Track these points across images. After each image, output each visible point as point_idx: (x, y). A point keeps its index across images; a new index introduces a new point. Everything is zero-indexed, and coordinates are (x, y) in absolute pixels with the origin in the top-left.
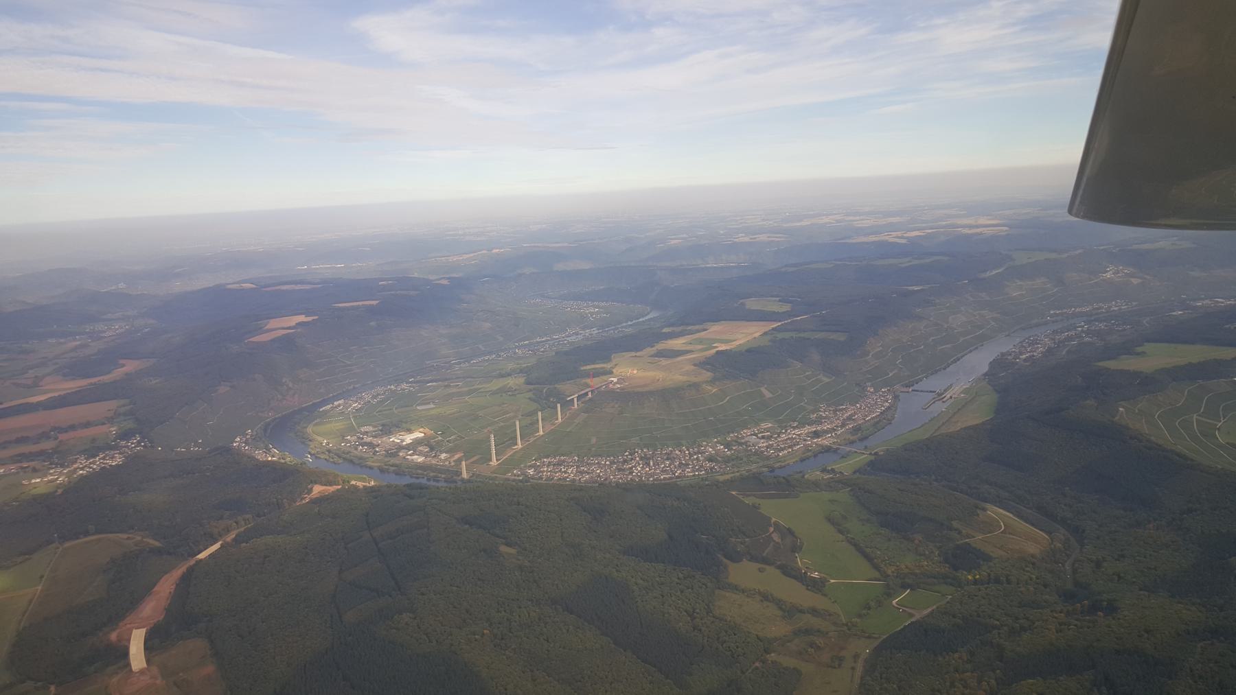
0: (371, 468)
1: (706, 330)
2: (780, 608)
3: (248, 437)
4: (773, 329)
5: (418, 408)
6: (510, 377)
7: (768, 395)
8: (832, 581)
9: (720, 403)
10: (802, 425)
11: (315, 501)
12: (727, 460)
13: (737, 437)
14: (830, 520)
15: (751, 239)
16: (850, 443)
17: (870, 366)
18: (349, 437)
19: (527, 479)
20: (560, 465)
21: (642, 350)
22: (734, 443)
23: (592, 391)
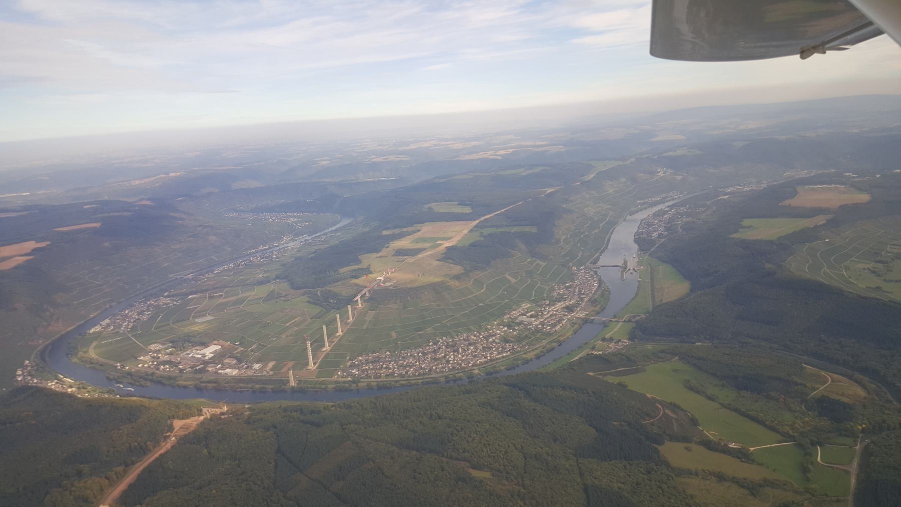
0: (185, 387)
1: (419, 231)
2: (743, 487)
3: (29, 368)
4: (475, 227)
5: (197, 320)
6: (269, 283)
7: (513, 280)
8: (752, 449)
9: (483, 291)
10: (553, 302)
11: (183, 441)
12: (519, 339)
13: (510, 318)
14: (691, 388)
15: (384, 159)
16: (598, 314)
17: (565, 251)
18: (142, 358)
20: (379, 362)
21: (380, 251)
22: (513, 324)
23: (369, 291)
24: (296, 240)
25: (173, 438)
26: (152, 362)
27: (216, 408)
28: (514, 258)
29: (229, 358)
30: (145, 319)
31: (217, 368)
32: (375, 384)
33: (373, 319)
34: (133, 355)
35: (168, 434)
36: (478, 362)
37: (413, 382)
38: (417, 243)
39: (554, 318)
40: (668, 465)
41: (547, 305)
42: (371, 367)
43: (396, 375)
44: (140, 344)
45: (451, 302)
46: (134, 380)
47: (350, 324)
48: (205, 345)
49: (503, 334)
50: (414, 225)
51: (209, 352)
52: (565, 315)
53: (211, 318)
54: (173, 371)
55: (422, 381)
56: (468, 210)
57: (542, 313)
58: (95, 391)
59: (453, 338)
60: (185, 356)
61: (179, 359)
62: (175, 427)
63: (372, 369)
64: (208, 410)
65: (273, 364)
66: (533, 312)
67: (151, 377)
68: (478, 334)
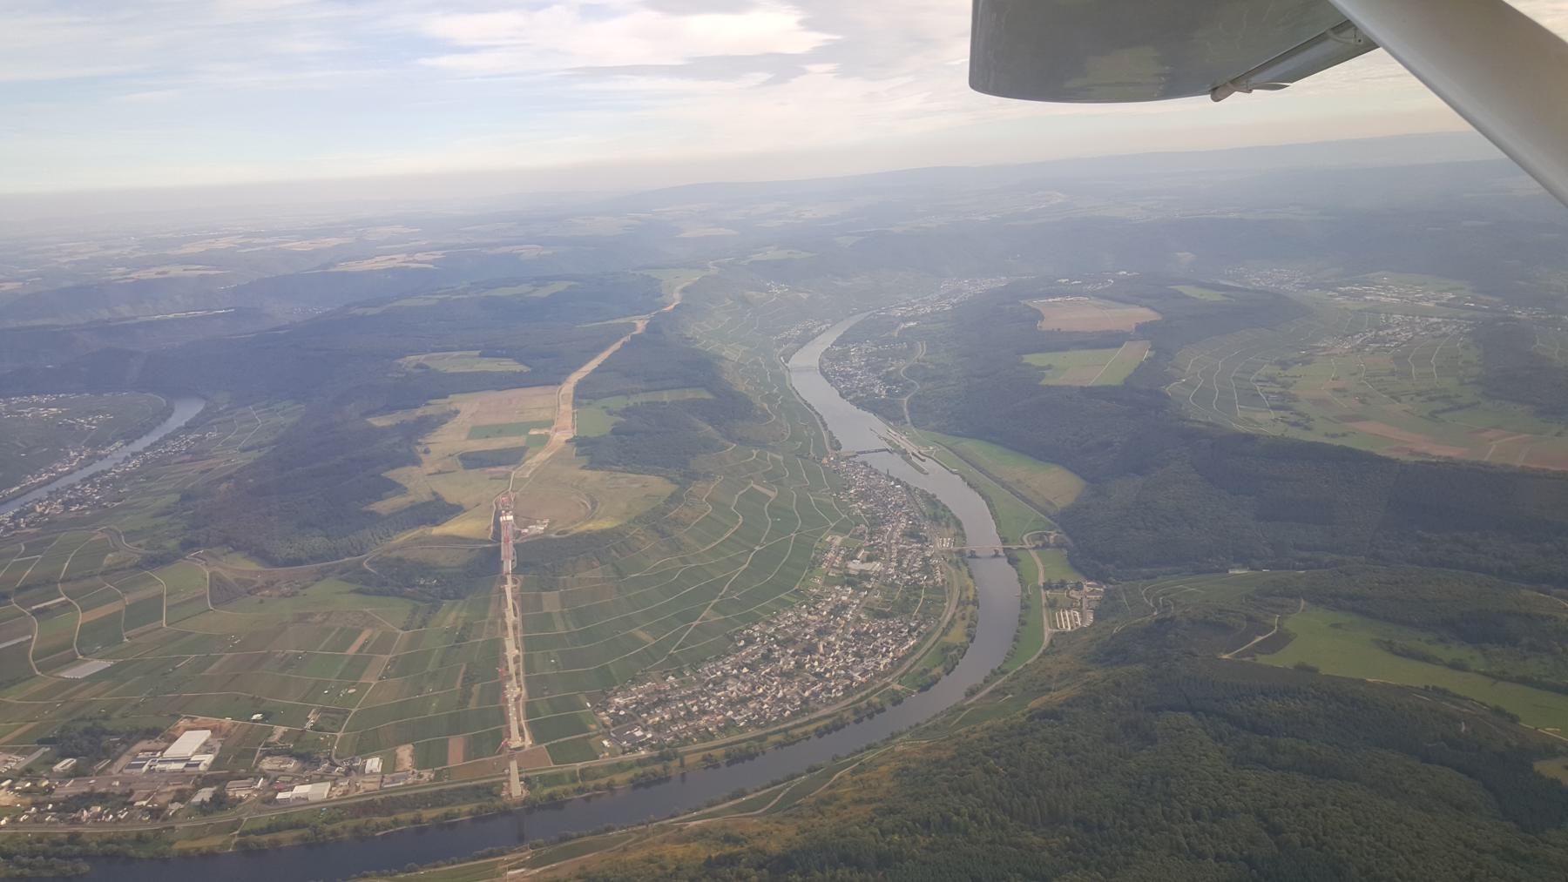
1: (457, 412)
15: (158, 273)
24: (106, 456)
29: (268, 759)
31: (258, 790)
32: (722, 751)
37: (797, 732)
42: (666, 717)
43: (741, 724)
50: (431, 401)
53: (106, 664)
56: (510, 366)
57: (882, 551)
63: (673, 721)
65: (408, 752)
68: (812, 609)
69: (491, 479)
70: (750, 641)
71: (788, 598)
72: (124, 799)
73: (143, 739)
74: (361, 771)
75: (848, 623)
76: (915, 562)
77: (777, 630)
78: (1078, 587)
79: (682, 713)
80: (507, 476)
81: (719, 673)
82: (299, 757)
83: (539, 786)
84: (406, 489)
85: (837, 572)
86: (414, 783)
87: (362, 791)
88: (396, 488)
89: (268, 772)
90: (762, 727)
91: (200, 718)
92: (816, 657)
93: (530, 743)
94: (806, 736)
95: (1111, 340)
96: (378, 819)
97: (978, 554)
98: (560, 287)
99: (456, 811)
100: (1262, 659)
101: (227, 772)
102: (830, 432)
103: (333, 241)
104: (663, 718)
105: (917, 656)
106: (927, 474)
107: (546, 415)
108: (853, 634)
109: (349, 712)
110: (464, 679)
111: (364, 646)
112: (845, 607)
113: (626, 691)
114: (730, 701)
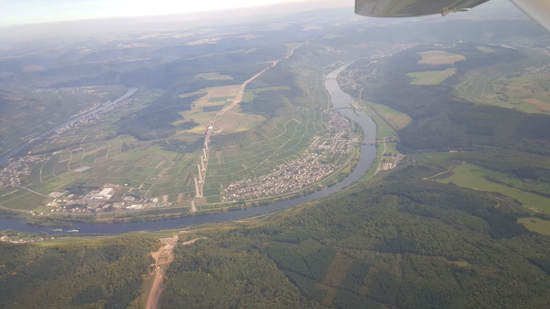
1: (207, 93)
15: (132, 46)
19: (241, 202)
24: (104, 105)
25: (159, 268)
26: (61, 206)
27: (168, 237)
28: (290, 107)
29: (127, 197)
30: (28, 173)
31: (122, 206)
32: (258, 202)
33: (222, 157)
34: (40, 202)
35: (152, 265)
36: (317, 179)
38: (214, 101)
39: (341, 144)
40: (540, 235)
41: (330, 136)
42: (244, 191)
43: (267, 194)
44: (40, 194)
45: (270, 140)
46: (56, 223)
47: (207, 162)
48: (99, 189)
49: (317, 158)
50: (200, 89)
51: (106, 192)
52: (346, 142)
53: (88, 168)
54: (85, 211)
55: (289, 196)
56: (229, 78)
57: (332, 142)
58: (26, 236)
59: (286, 164)
60: (87, 198)
61: (84, 202)
62: (155, 258)
63: (246, 192)
64: (163, 240)
65: (166, 197)
66: (325, 142)
67: (69, 219)
68: (301, 160)
69: (210, 115)
70: (278, 169)
71: (294, 156)
72: (84, 206)
73: (93, 190)
74: (151, 202)
75: (312, 165)
76: (342, 146)
77: (288, 166)
78: (395, 155)
79: (250, 190)
80: (215, 115)
81: (265, 179)
82: (135, 197)
83: (201, 209)
84: (184, 118)
85: (314, 148)
86: (166, 206)
87: (150, 207)
88: (181, 117)
89: (125, 201)
90: (273, 196)
91: (110, 184)
92: (297, 175)
93: (202, 196)
94: (286, 199)
95: (443, 67)
96: (153, 216)
97: (366, 144)
98: (253, 50)
99: (175, 215)
100: (438, 181)
101: (114, 200)
102: (331, 101)
103: (188, 34)
104: (243, 191)
105: (331, 176)
106: (359, 116)
107: (234, 94)
108: (312, 169)
109: (152, 185)
110: (187, 176)
111: (161, 165)
112: (313, 160)
113: (235, 182)
114: (266, 187)
